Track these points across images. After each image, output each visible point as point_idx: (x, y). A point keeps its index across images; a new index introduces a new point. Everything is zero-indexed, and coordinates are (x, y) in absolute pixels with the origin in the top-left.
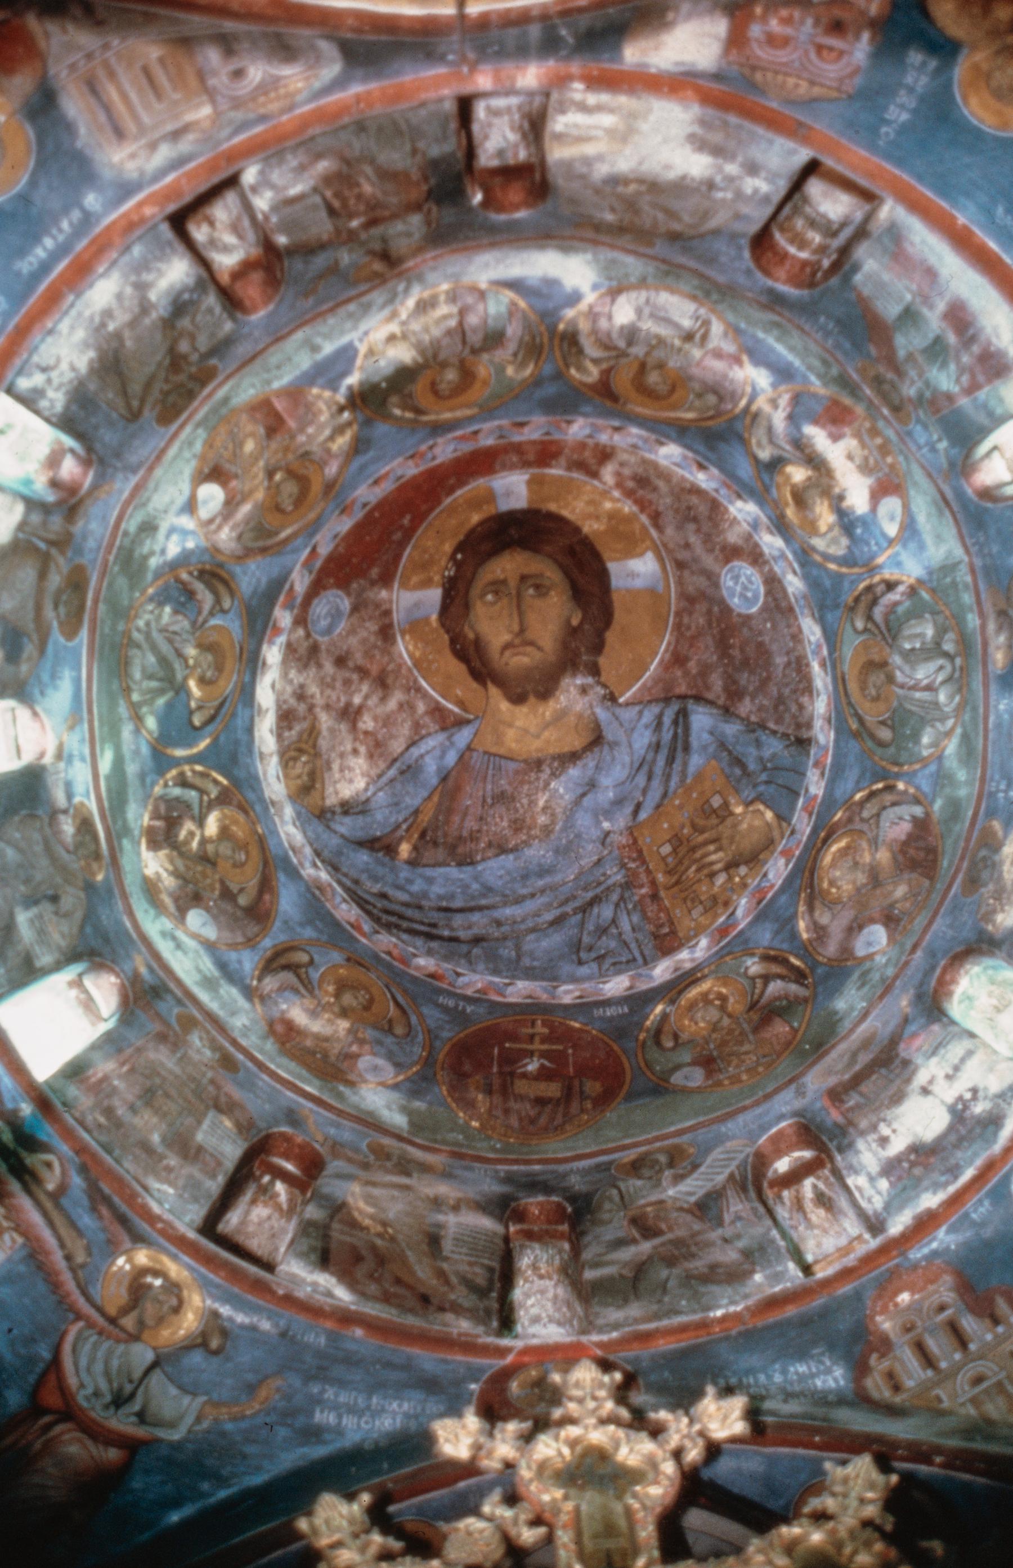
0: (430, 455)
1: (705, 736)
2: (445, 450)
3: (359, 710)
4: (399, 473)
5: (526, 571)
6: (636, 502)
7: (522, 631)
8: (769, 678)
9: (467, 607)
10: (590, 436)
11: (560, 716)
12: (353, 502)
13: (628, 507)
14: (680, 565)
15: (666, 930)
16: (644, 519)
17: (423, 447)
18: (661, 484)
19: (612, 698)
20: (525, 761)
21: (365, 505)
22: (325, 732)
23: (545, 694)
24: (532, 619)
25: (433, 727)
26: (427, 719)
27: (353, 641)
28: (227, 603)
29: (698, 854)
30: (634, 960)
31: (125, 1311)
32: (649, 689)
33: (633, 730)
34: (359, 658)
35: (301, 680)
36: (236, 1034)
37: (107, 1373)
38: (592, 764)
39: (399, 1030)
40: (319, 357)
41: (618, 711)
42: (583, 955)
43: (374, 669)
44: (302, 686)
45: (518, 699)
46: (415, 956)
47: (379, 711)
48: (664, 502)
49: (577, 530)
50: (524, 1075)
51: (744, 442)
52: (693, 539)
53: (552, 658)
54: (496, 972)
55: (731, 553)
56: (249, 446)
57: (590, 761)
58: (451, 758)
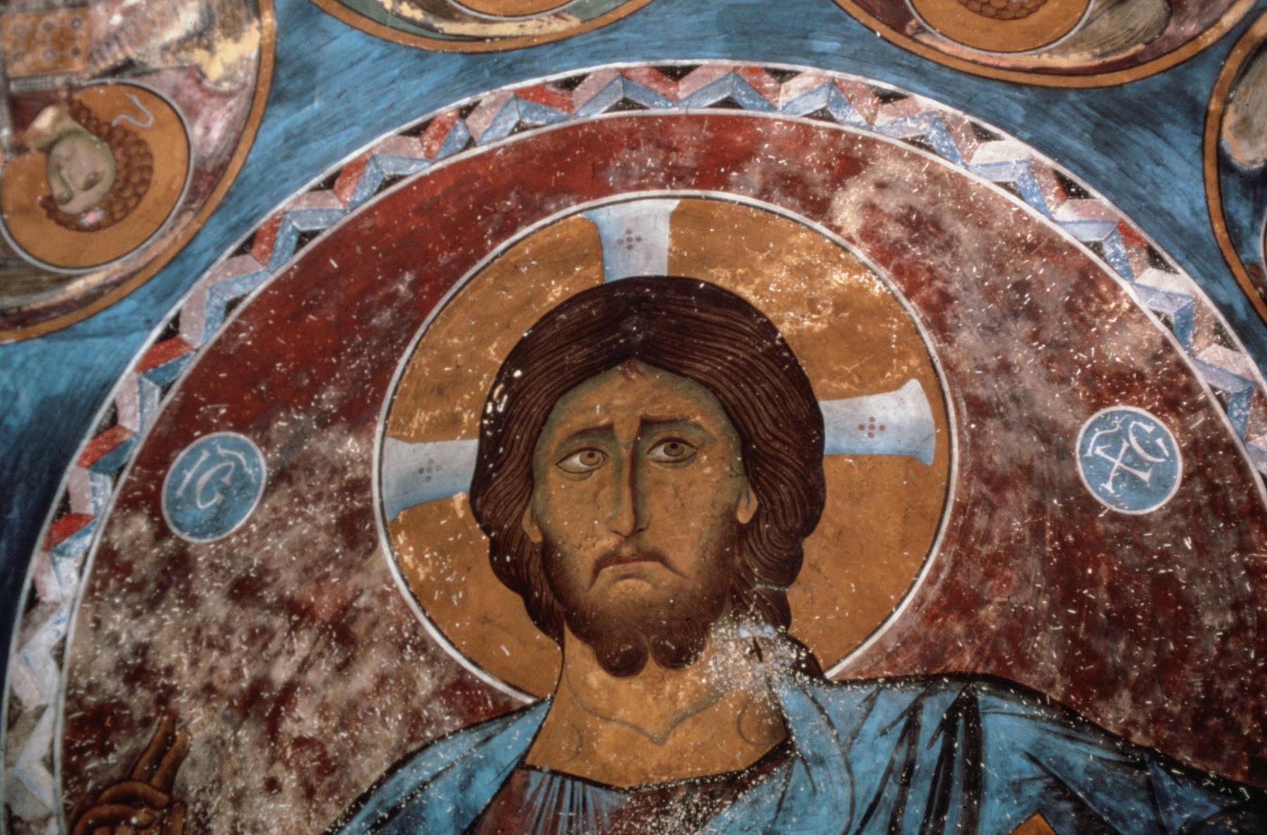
0: (461, 133)
1: (1020, 763)
2: (498, 124)
3: (288, 693)
4: (389, 169)
5: (654, 412)
6: (899, 273)
7: (637, 530)
8: (1183, 655)
9: (530, 480)
10: (823, 115)
11: (706, 701)
12: (274, 227)
13: (881, 284)
14: (980, 409)
16: (912, 309)
17: (447, 111)
18: (963, 231)
19: (813, 669)
20: (636, 792)
21: (304, 238)
22: (197, 749)
23: (677, 659)
24: (656, 508)
25: (451, 723)
26: (437, 707)
27: (277, 546)
32: (891, 657)
33: (855, 735)
34: (290, 583)
35: (141, 634)
38: (770, 800)
41: (824, 694)
43: (325, 606)
44: (142, 649)
45: (625, 666)
47: (336, 693)
48: (965, 273)
49: (769, 329)
51: (1199, 118)
52: (1019, 355)
53: (695, 584)
55: (1114, 384)
57: (766, 792)
58: (485, 788)
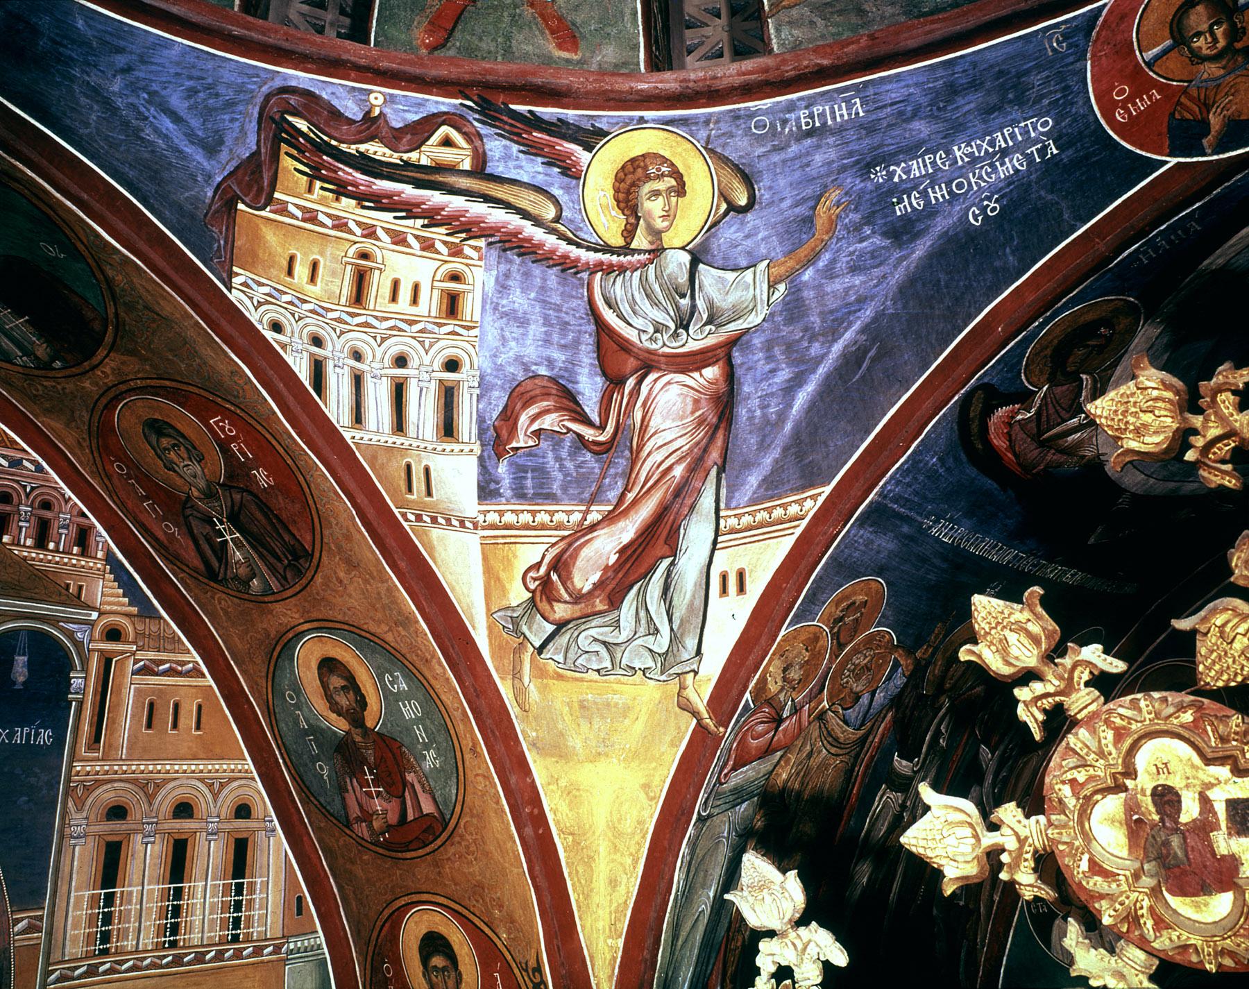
31: (629, 233)
37: (655, 303)
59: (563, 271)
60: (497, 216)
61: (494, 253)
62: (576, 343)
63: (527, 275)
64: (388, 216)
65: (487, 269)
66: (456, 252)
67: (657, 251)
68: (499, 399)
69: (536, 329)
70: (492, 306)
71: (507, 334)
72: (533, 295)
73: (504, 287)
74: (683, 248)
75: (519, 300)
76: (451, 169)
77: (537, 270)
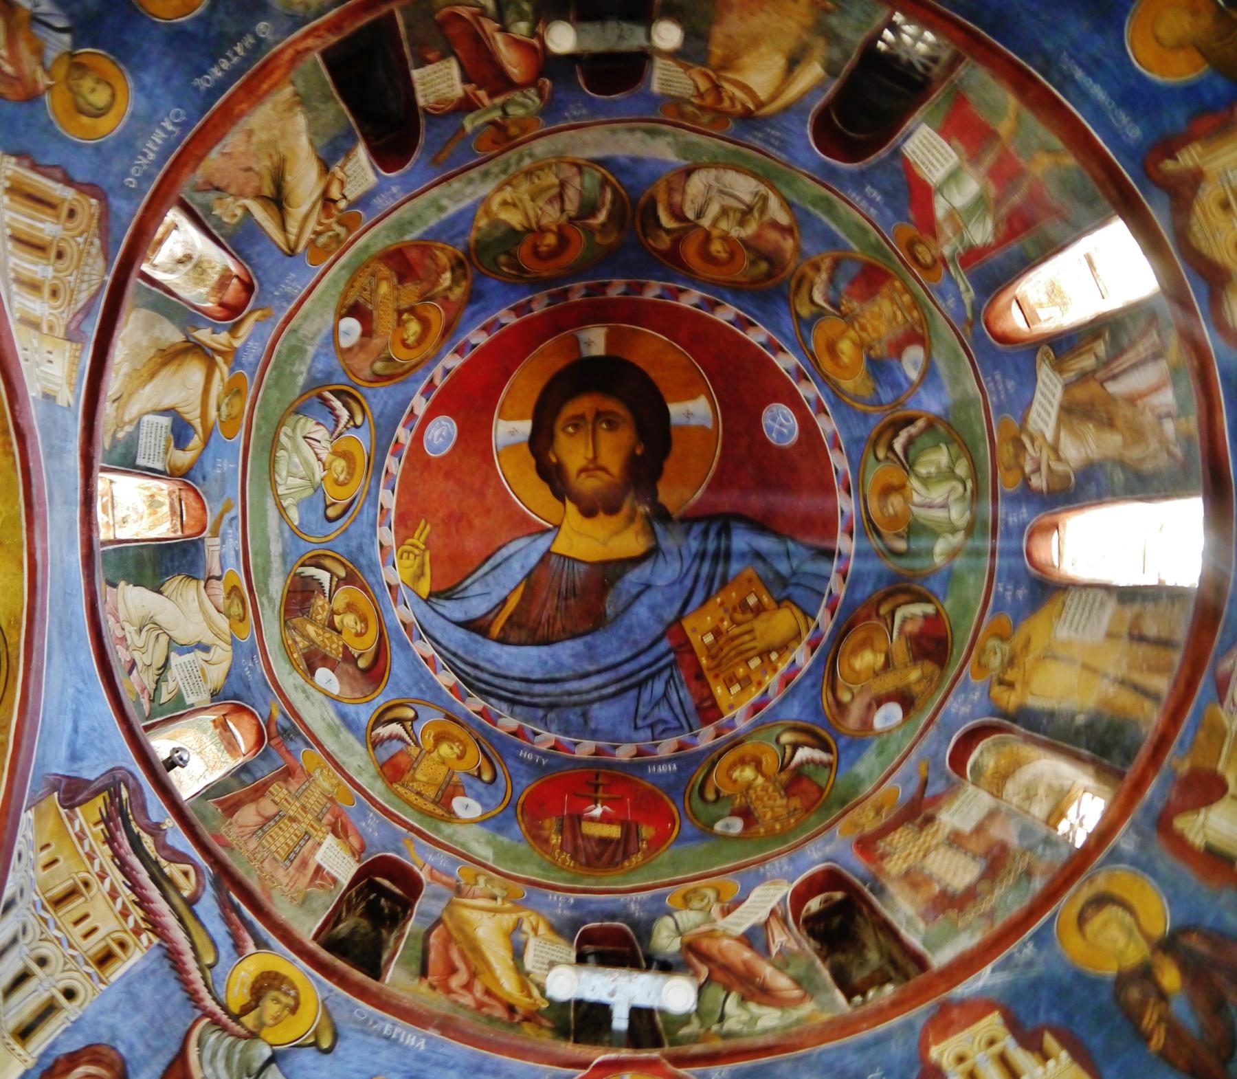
5: (602, 409)
7: (595, 457)
9: (551, 438)
15: (707, 704)
28: (359, 420)
29: (737, 642)
30: (682, 727)
31: (246, 1010)
36: (351, 773)
39: (486, 777)
40: (444, 216)
42: (640, 723)
46: (500, 716)
50: (592, 820)
54: (566, 733)
56: (384, 288)
58: (534, 558)
59: (189, 999)
60: (178, 935)
61: (158, 952)
62: (157, 1051)
63: (165, 982)
64: (120, 877)
65: (145, 958)
66: (137, 932)
67: (253, 1035)
68: (77, 1043)
69: (140, 1020)
70: (129, 982)
71: (121, 1006)
72: (158, 997)
73: (145, 977)
74: (271, 1045)
75: (146, 991)
76: (177, 889)
77: (174, 985)
